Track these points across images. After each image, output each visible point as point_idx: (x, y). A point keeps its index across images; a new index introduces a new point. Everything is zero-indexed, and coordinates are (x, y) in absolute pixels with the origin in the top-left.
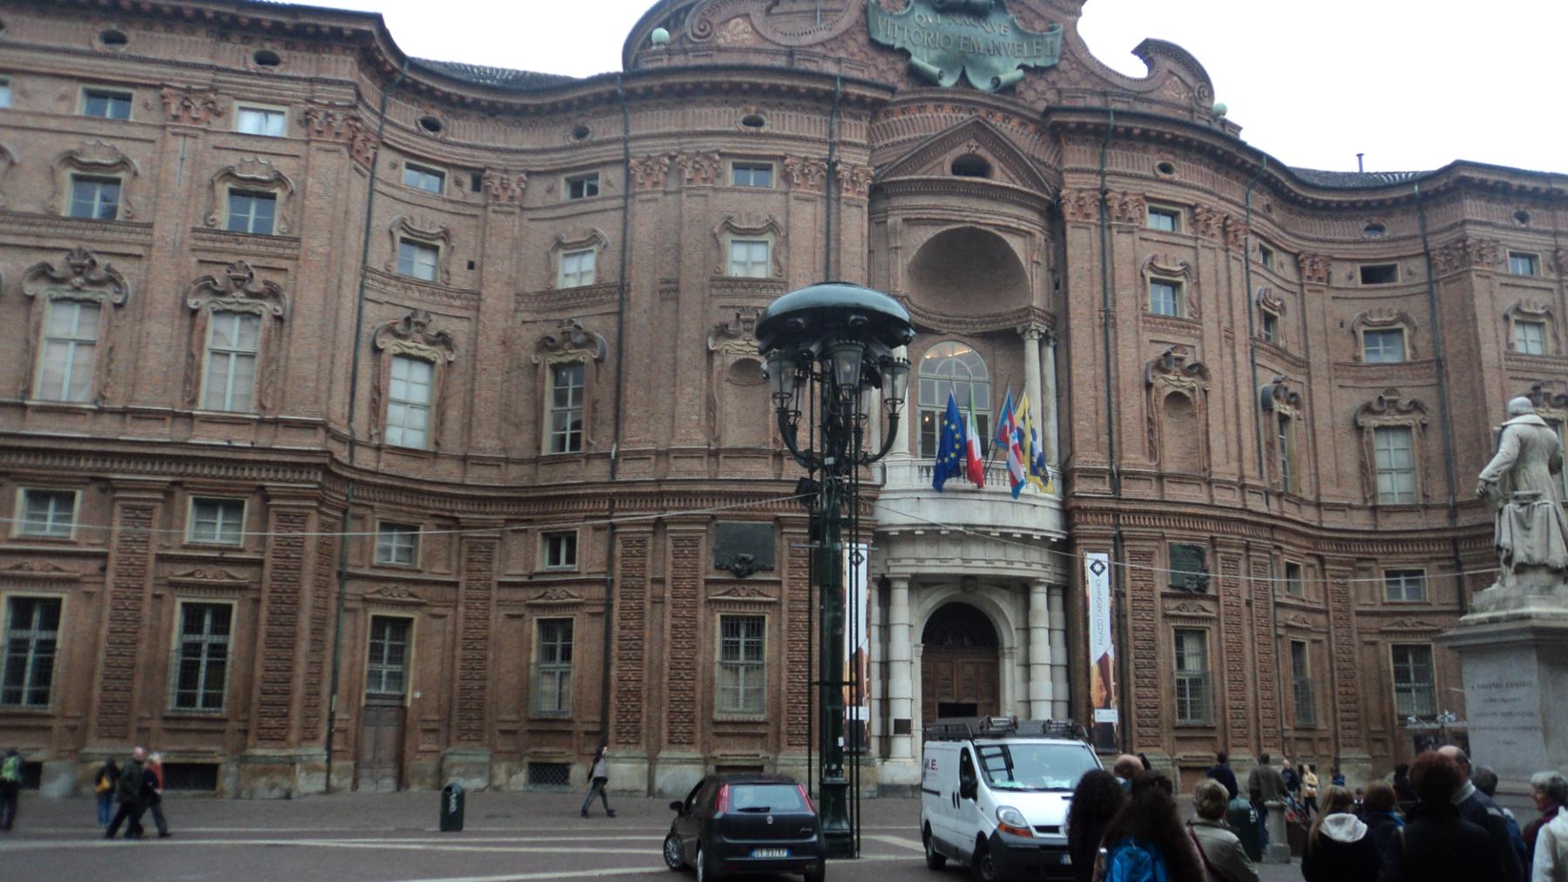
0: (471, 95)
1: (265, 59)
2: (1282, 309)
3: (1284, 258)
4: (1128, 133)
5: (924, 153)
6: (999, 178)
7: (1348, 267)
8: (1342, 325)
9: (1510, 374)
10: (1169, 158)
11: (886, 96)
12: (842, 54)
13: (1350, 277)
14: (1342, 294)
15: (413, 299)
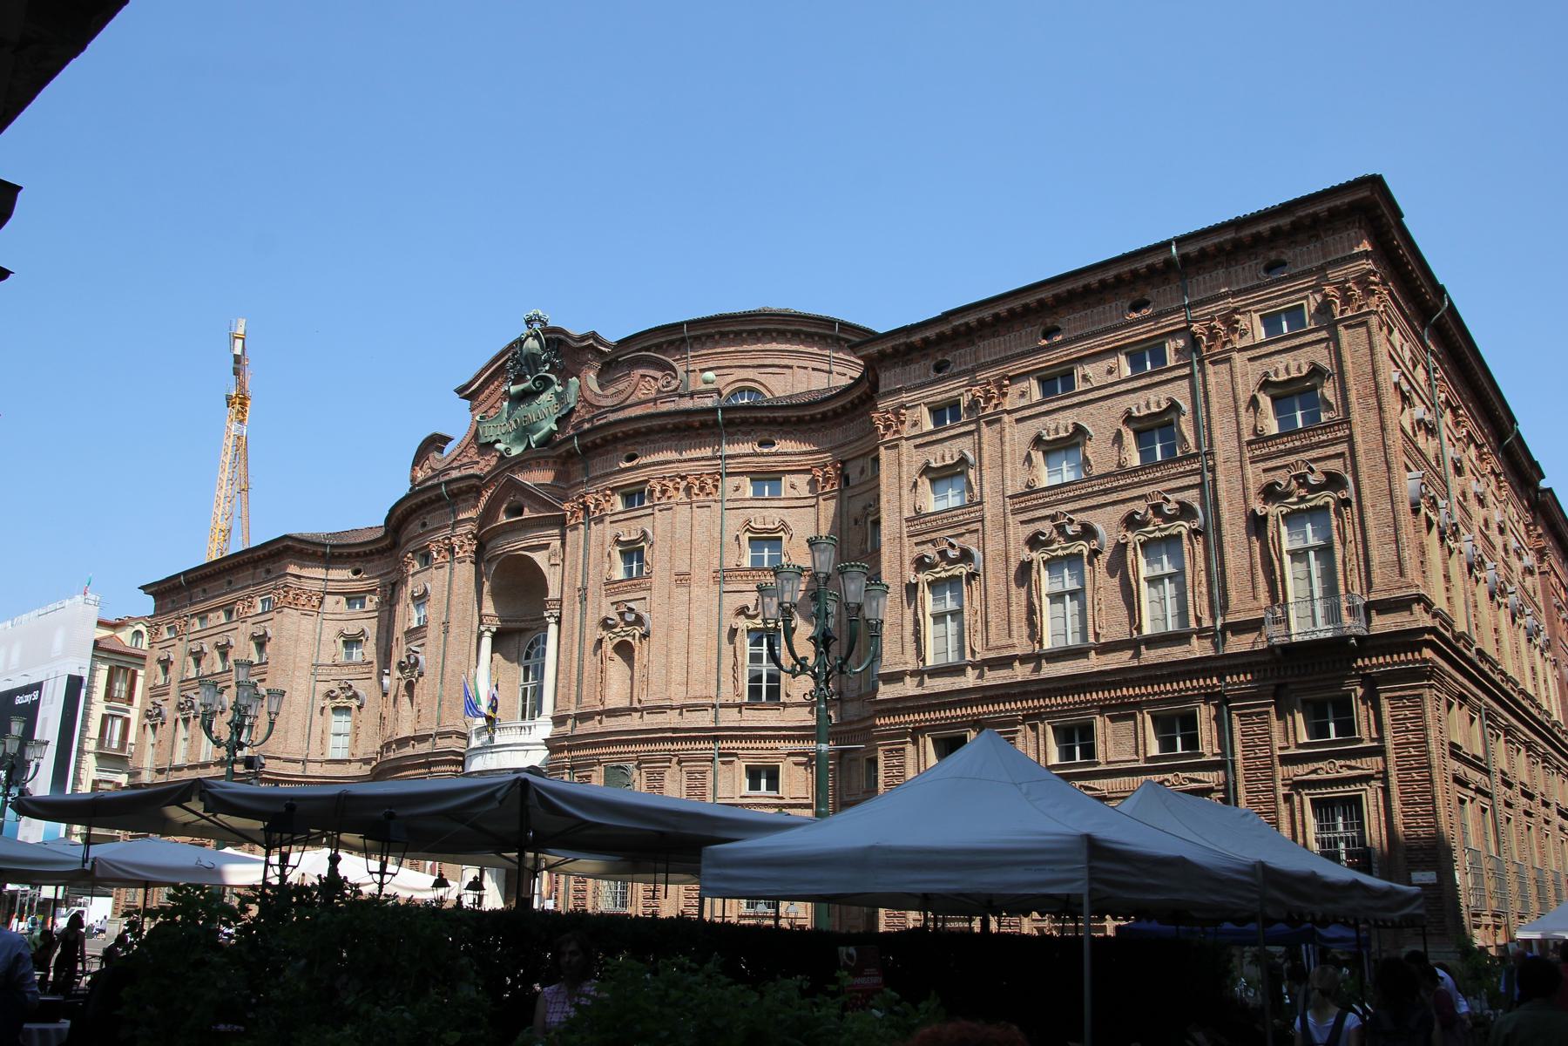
0: (367, 549)
1: (268, 571)
2: (784, 526)
3: (794, 478)
4: (595, 446)
5: (489, 514)
6: (527, 514)
7: (860, 462)
8: (856, 522)
9: (915, 540)
10: (631, 450)
11: (474, 481)
12: (466, 460)
13: (862, 472)
14: (857, 491)
15: (344, 674)
